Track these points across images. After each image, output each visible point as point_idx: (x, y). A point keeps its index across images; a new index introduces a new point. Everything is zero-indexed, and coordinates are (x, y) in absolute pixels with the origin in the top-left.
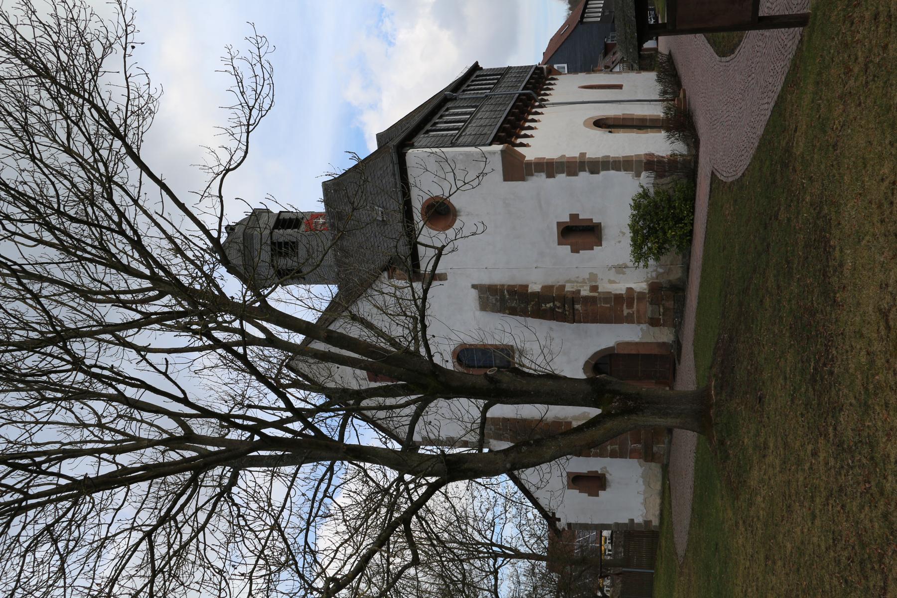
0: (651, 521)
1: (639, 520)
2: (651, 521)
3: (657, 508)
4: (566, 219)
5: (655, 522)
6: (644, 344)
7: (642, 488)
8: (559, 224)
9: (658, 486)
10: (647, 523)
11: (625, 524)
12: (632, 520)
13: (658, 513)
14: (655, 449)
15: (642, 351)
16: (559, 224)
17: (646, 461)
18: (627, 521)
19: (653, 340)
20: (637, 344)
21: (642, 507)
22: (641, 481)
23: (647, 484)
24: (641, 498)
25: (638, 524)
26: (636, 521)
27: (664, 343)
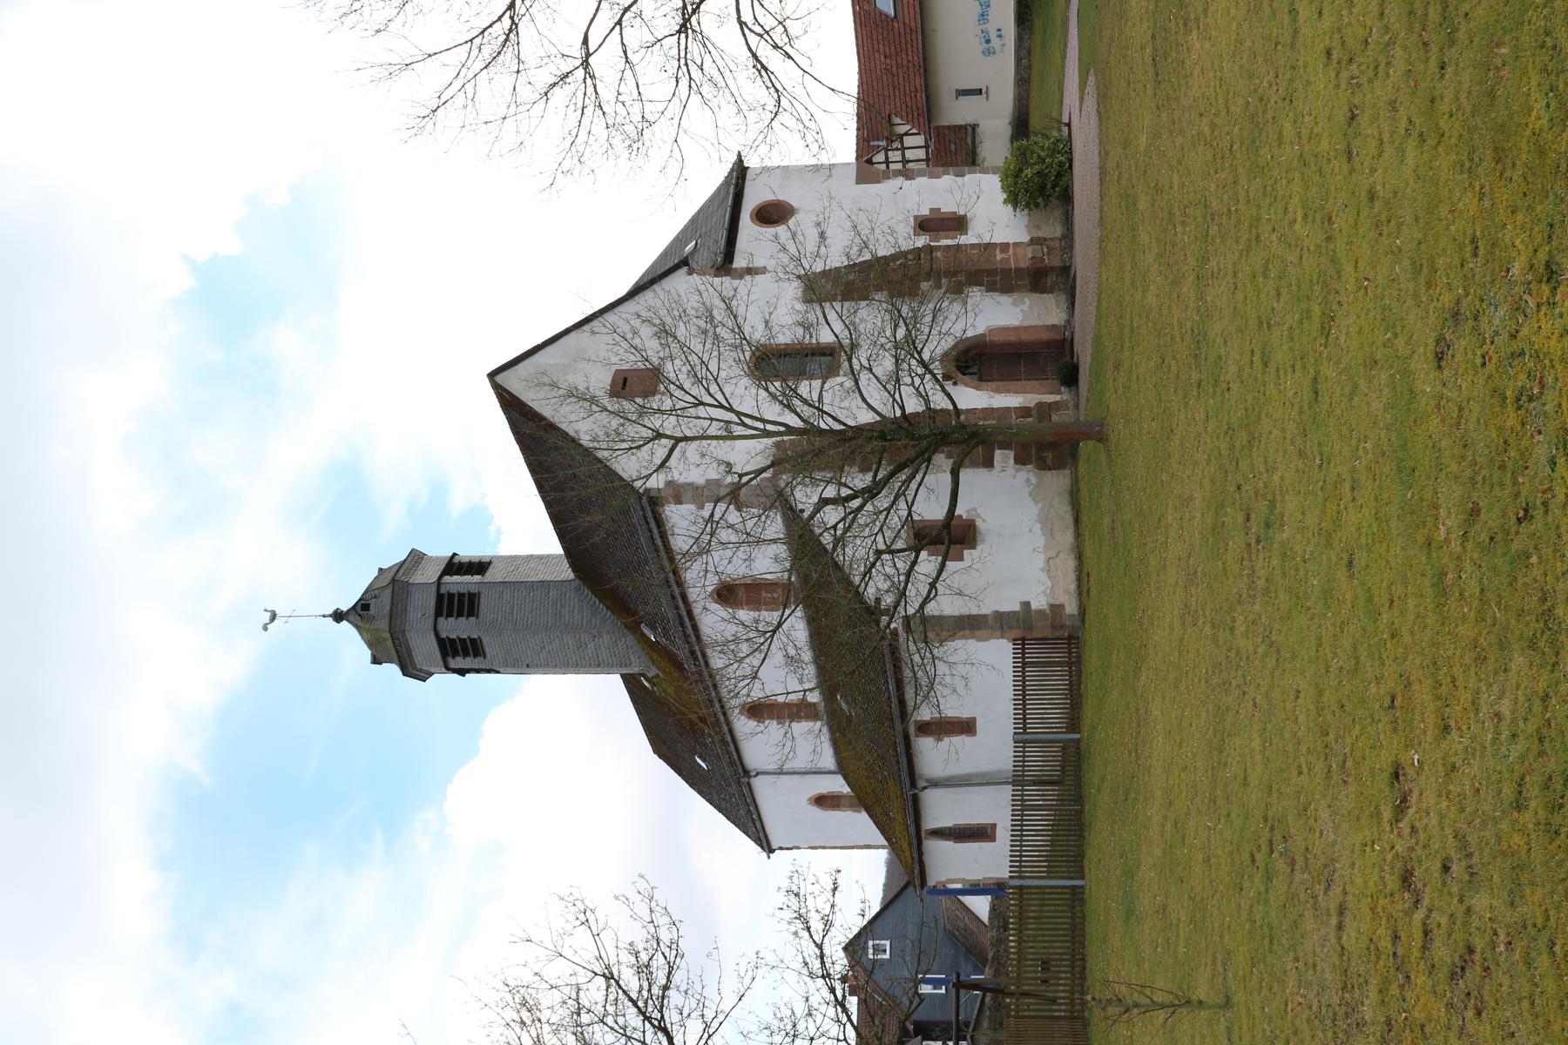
0: (1061, 606)
1: (1039, 603)
2: (1061, 606)
3: (1072, 576)
4: (925, 212)
5: (1071, 608)
6: (1027, 328)
7: (1040, 541)
8: (916, 217)
9: (1068, 537)
10: (1056, 609)
11: (1014, 613)
12: (1027, 604)
13: (1073, 587)
14: (1054, 418)
15: (1025, 337)
16: (916, 217)
17: (1043, 466)
18: (1016, 607)
19: (1038, 323)
20: (1016, 328)
21: (1044, 577)
22: (1037, 528)
23: (1049, 532)
24: (1040, 561)
25: (1039, 612)
26: (1034, 606)
27: (1054, 326)
